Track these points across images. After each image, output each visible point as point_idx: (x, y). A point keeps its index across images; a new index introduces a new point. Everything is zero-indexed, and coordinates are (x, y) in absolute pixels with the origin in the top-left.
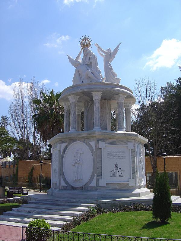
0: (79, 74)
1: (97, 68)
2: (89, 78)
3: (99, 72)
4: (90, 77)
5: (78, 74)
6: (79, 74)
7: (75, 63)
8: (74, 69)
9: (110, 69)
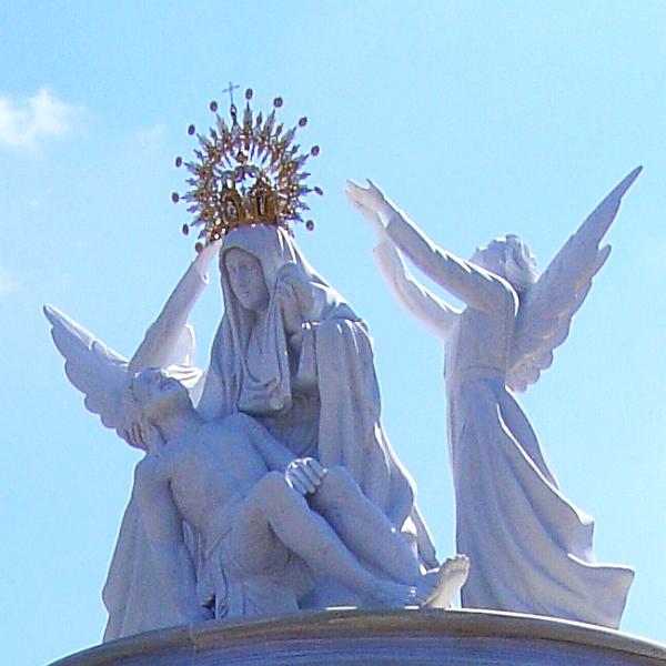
0: (180, 518)
1: (371, 452)
2: (281, 558)
3: (398, 498)
4: (291, 556)
5: (166, 519)
6: (180, 518)
7: (128, 396)
8: (114, 465)
9: (512, 463)
